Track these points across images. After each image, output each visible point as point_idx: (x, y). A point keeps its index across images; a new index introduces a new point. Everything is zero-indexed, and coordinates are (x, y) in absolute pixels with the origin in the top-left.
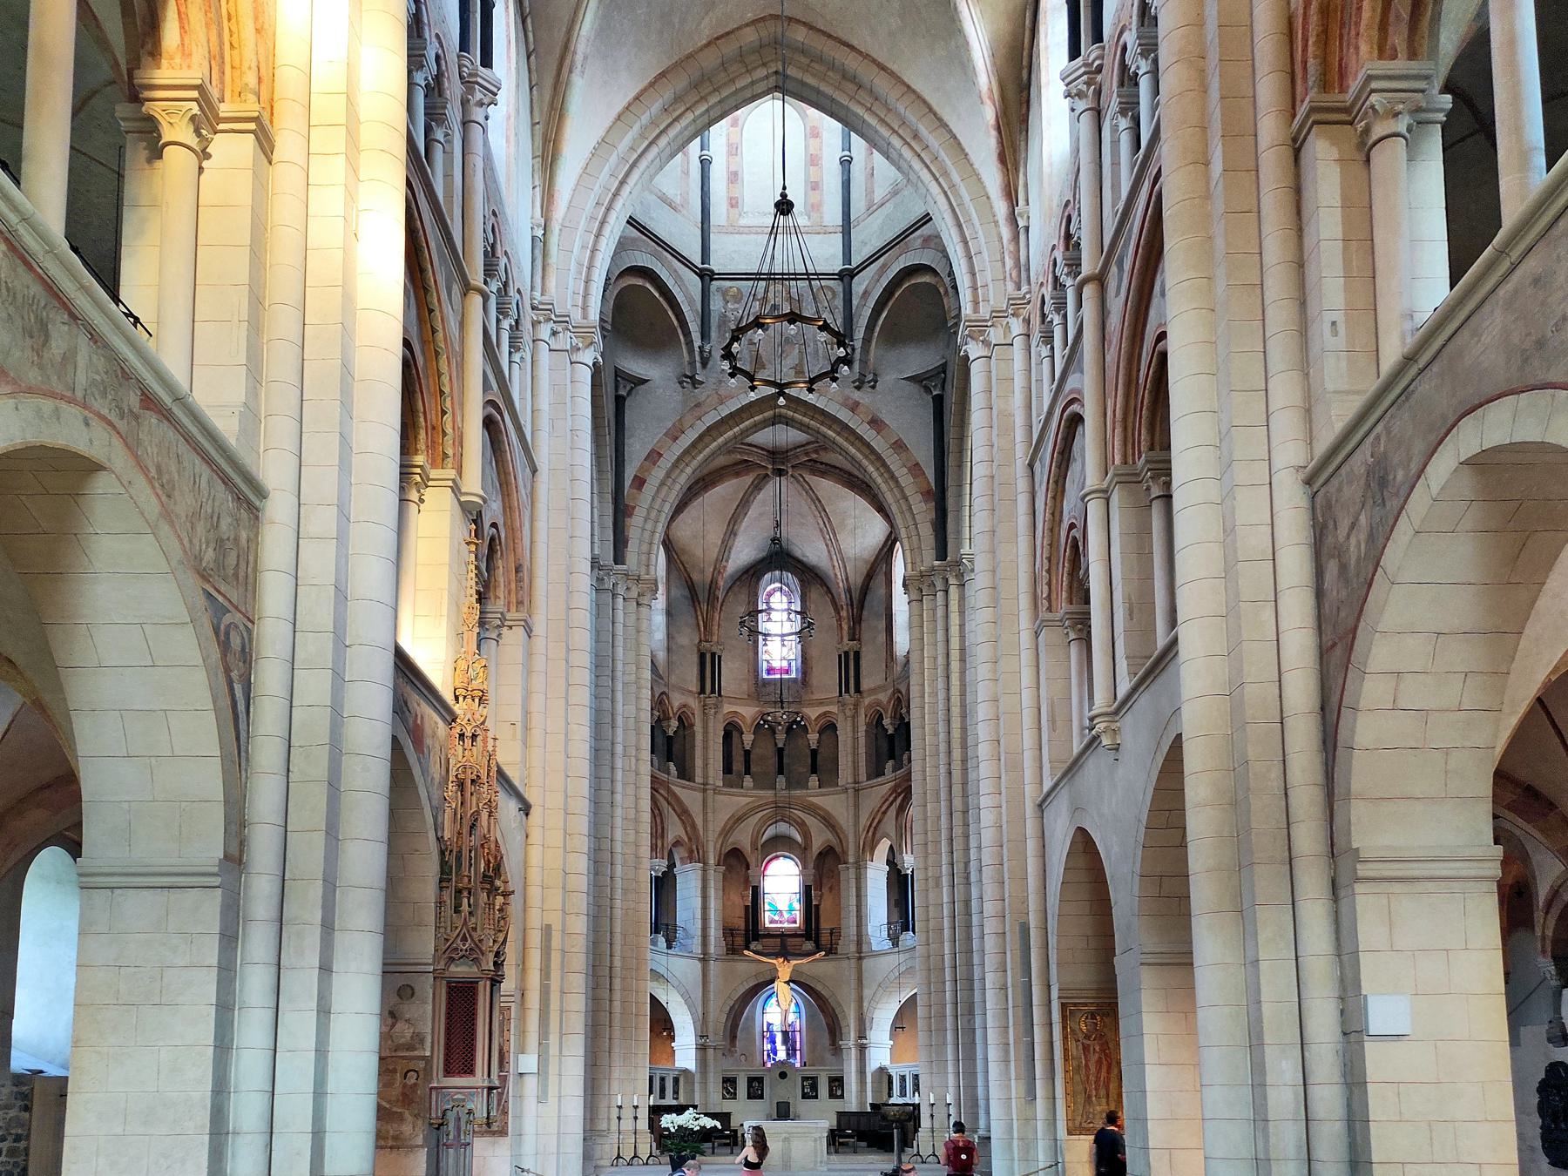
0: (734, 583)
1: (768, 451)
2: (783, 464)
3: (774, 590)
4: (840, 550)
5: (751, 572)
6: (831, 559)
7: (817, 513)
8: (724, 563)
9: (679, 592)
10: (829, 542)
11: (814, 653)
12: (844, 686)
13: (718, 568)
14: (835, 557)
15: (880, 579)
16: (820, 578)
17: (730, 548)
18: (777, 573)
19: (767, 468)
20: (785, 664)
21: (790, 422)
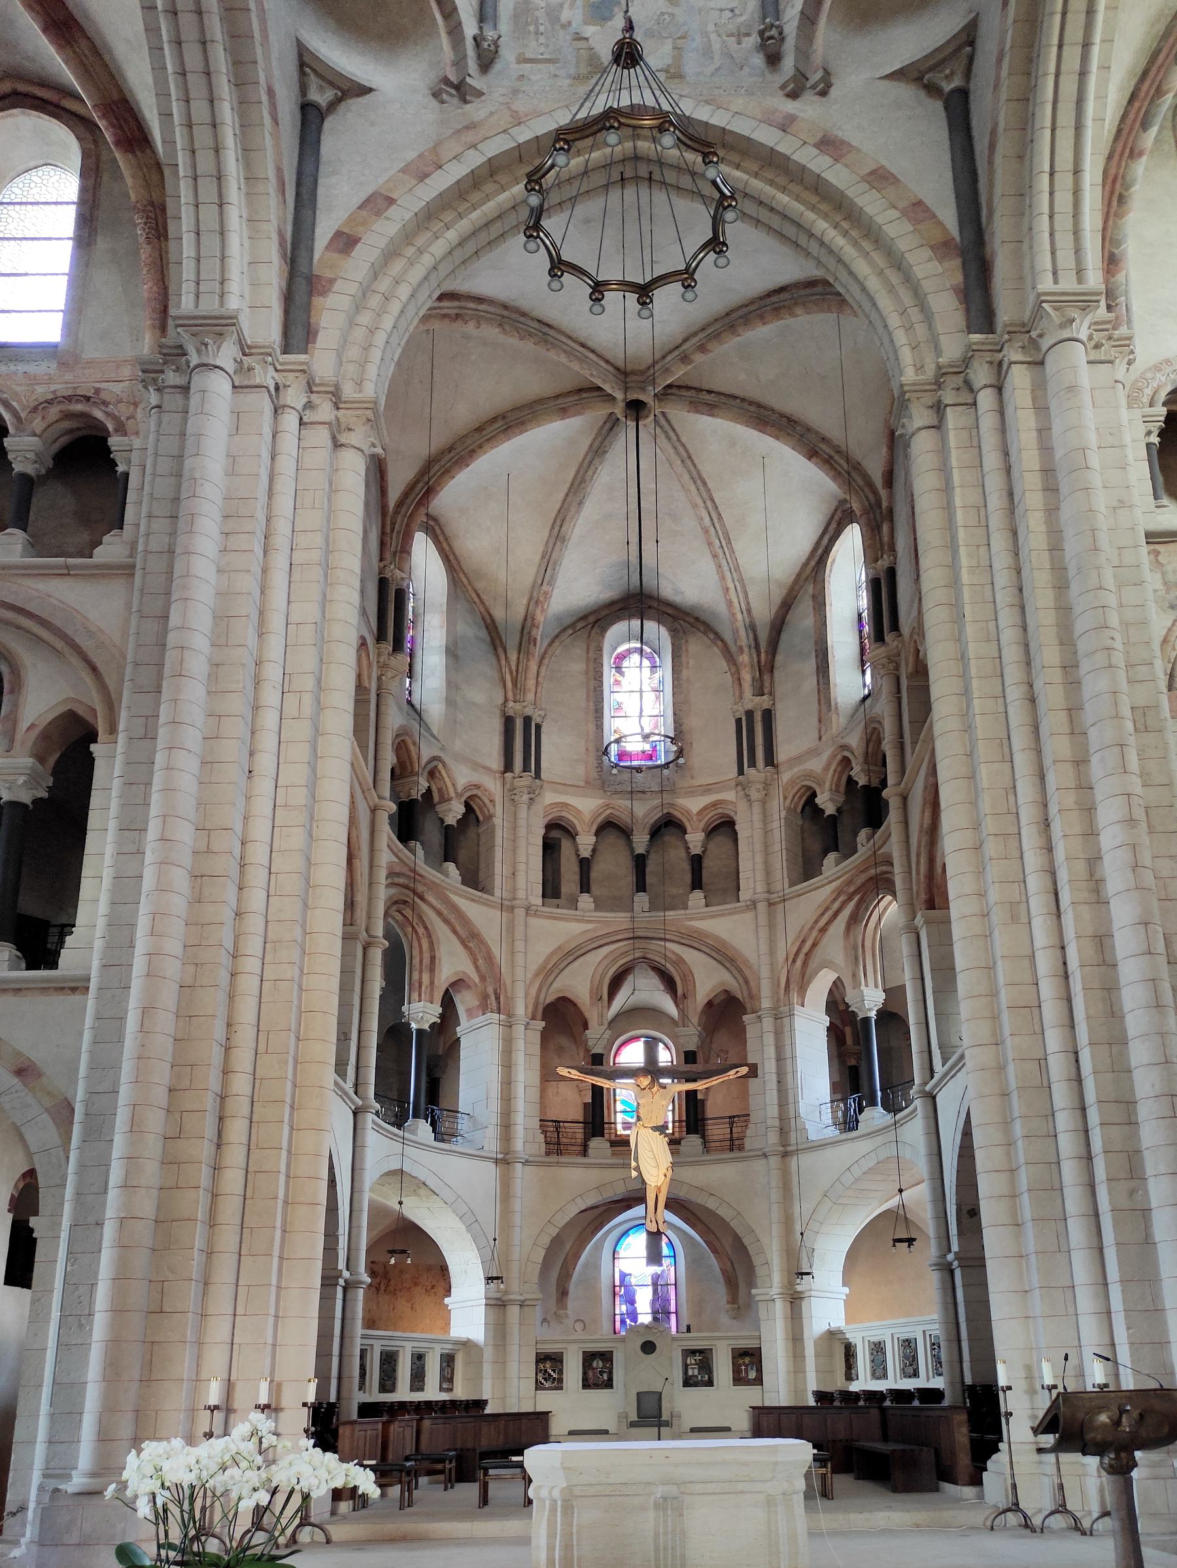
0: (564, 630)
1: (617, 369)
2: (643, 389)
3: (629, 652)
4: (737, 568)
5: (592, 619)
6: (723, 578)
7: (699, 501)
8: (545, 588)
9: (470, 630)
10: (720, 551)
11: (693, 722)
12: (744, 758)
13: (536, 598)
14: (728, 575)
15: (805, 607)
16: (704, 623)
17: (555, 563)
18: (636, 623)
19: (611, 399)
20: (647, 747)
21: (657, 176)
